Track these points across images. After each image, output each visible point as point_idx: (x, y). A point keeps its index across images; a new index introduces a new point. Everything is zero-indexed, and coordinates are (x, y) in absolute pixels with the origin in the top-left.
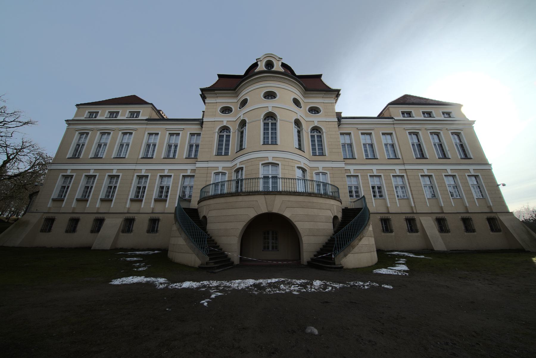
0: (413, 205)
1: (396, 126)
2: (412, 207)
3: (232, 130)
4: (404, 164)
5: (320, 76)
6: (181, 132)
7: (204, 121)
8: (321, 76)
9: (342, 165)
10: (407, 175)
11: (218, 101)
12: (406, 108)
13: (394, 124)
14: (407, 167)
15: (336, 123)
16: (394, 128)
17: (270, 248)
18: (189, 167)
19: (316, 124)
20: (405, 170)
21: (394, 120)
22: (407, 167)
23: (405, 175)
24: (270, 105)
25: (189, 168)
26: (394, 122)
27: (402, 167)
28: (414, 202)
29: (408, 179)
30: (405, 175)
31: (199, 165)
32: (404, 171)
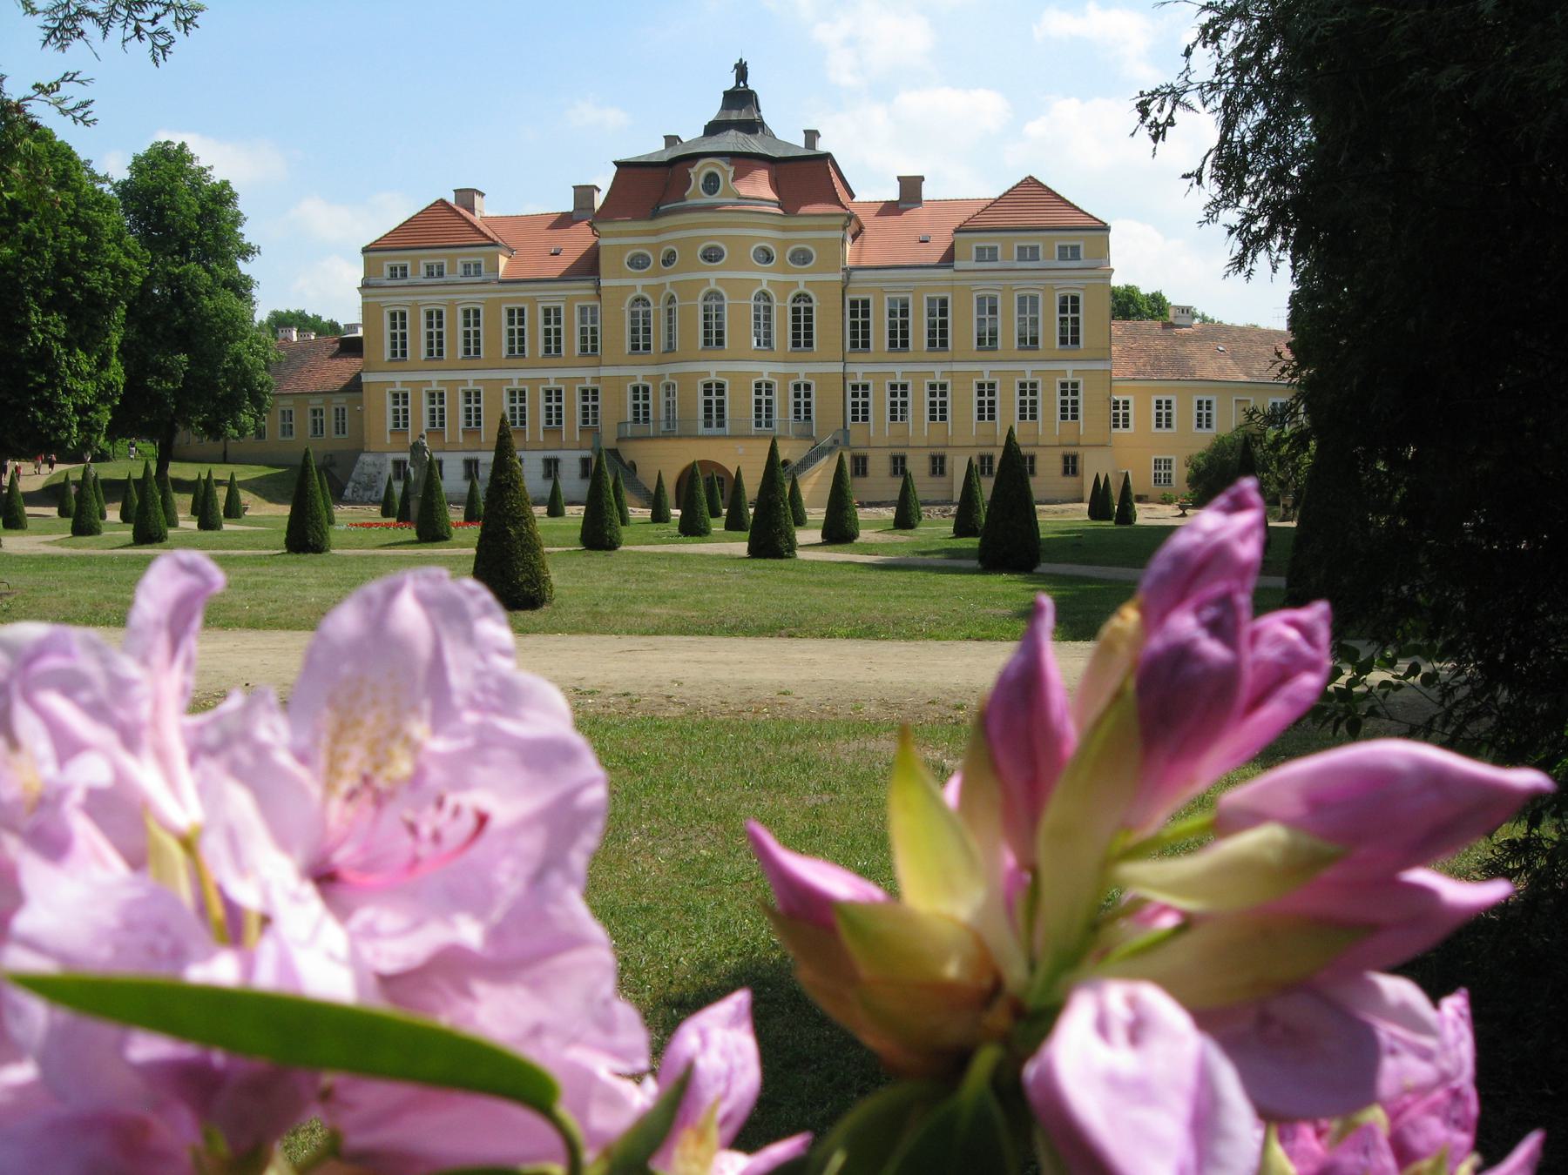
1: (956, 283)
7: (602, 285)
10: (952, 383)
12: (986, 240)
15: (840, 286)
16: (953, 286)
18: (588, 373)
19: (802, 289)
21: (952, 270)
22: (956, 367)
23: (949, 381)
24: (713, 276)
25: (586, 375)
27: (947, 367)
28: (952, 429)
30: (949, 381)
31: (605, 372)
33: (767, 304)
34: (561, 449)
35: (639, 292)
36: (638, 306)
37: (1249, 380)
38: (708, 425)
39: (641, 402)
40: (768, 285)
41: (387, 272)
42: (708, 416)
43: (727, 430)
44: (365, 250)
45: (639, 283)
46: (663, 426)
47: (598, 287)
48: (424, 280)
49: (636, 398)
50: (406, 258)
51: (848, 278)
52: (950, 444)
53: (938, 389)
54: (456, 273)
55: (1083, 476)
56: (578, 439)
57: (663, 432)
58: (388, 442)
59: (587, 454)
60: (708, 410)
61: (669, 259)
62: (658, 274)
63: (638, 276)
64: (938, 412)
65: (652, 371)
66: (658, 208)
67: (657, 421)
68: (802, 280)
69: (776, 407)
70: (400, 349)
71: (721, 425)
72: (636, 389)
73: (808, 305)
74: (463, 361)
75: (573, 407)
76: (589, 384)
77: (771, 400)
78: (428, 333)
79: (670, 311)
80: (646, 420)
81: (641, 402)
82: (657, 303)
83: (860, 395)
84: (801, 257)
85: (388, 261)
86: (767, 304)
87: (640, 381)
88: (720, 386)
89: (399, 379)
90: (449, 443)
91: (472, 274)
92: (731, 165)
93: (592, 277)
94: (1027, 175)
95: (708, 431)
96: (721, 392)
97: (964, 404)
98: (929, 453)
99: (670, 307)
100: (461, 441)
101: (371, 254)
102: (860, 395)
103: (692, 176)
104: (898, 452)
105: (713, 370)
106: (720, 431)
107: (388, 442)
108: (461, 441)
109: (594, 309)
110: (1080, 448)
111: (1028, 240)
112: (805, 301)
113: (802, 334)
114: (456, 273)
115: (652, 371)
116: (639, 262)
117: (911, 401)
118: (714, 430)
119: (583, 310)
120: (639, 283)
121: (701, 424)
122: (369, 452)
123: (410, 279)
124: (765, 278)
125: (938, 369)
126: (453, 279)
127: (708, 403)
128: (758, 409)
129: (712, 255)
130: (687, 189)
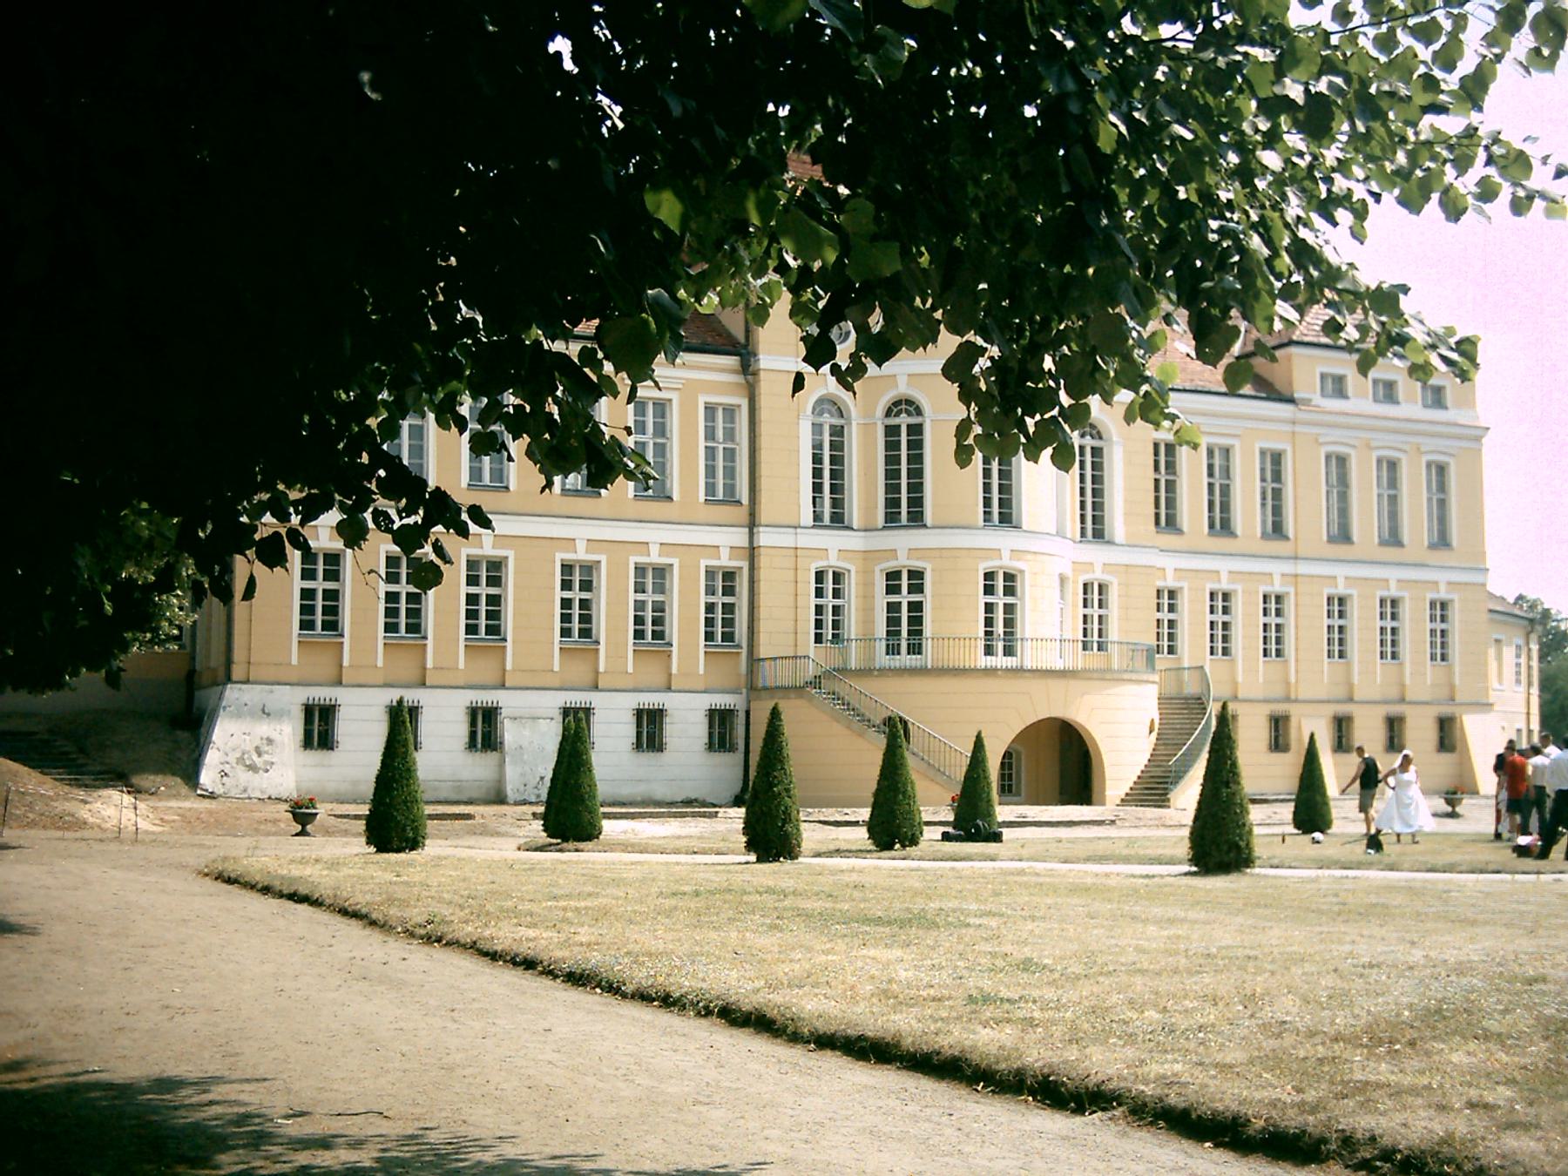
0: (1293, 680)
1: (1298, 429)
4: (1296, 558)
20: (1296, 576)
22: (1303, 568)
27: (1288, 568)
28: (1297, 671)
39: (829, 601)
53: (1275, 603)
59: (722, 701)
73: (1096, 443)
76: (725, 561)
77: (733, 605)
81: (829, 601)
87: (833, 561)
95: (990, 661)
98: (1384, 713)
99: (893, 421)
106: (1010, 662)
109: (730, 412)
119: (710, 410)
122: (247, 682)
125: (1277, 568)
128: (989, 622)
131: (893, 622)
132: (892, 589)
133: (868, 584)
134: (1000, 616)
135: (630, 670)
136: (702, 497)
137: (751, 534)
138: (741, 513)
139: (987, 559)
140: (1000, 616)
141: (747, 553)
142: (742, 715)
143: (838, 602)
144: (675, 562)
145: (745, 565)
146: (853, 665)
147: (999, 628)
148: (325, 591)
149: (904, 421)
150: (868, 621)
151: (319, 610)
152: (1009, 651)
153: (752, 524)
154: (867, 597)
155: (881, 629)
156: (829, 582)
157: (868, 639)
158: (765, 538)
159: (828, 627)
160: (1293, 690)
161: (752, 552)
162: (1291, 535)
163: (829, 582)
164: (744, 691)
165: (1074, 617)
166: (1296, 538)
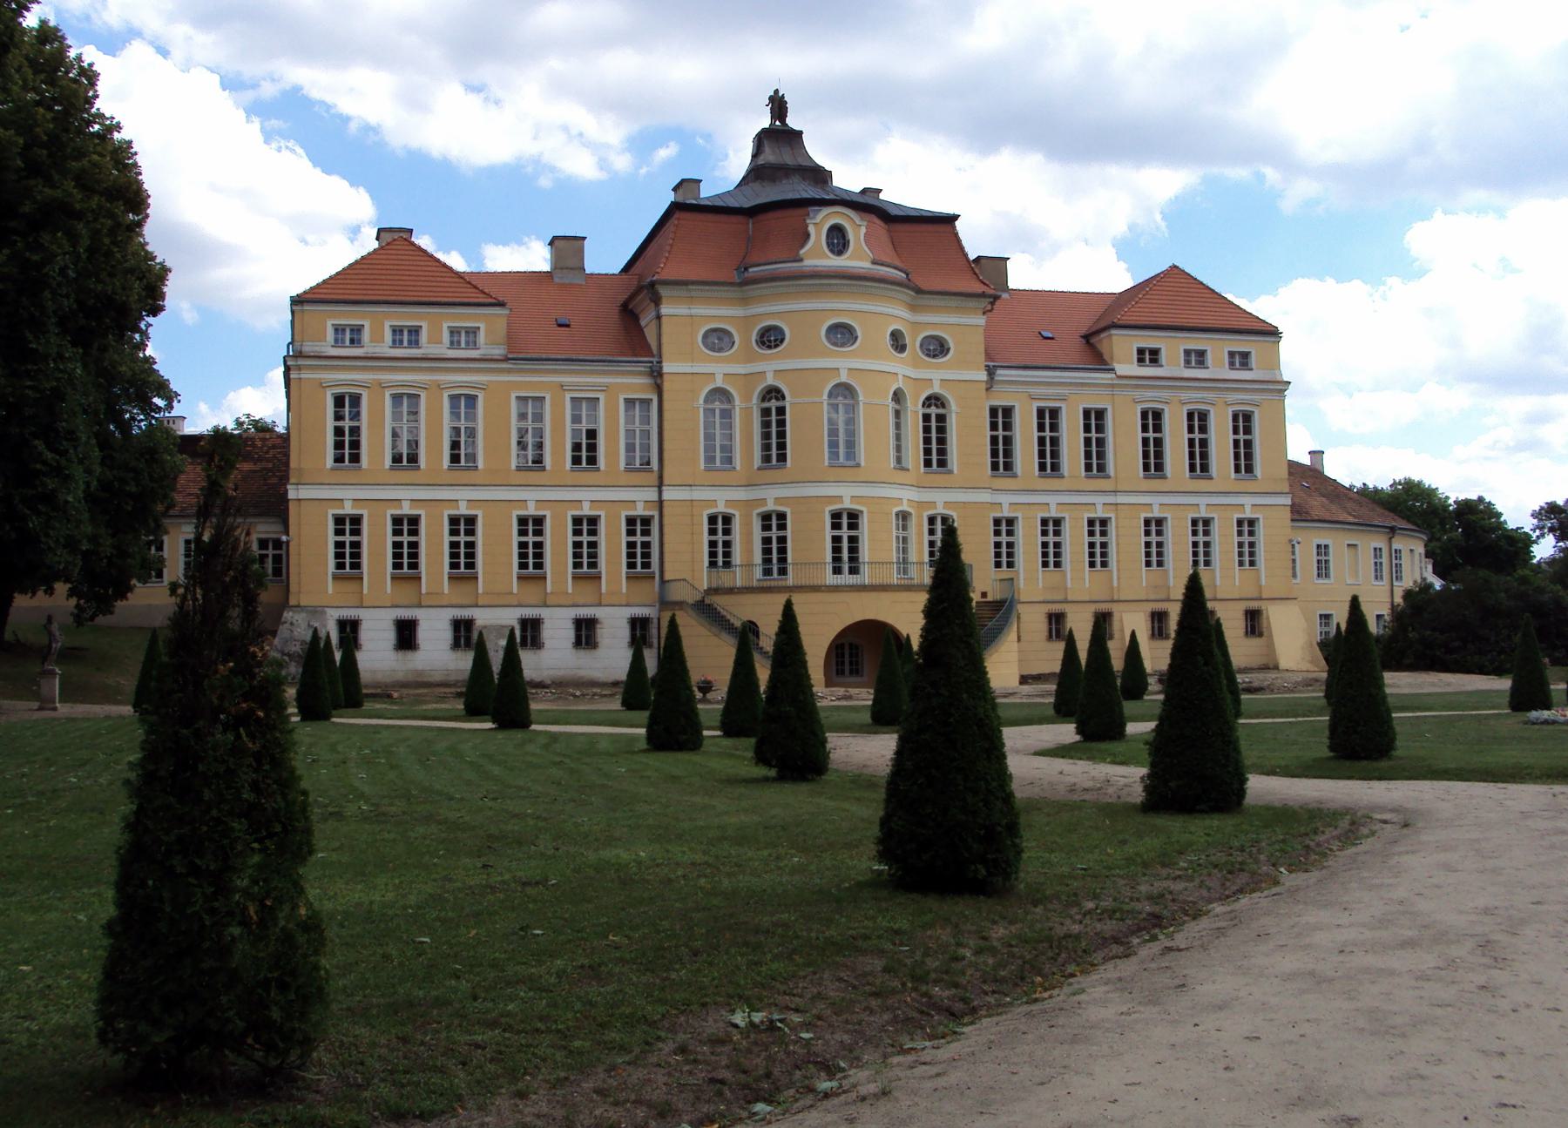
0: (1115, 584)
1: (1117, 391)
2: (1112, 588)
3: (737, 402)
5: (952, 219)
6: (601, 396)
7: (665, 370)
8: (956, 217)
9: (985, 497)
10: (1117, 518)
11: (693, 312)
13: (1113, 386)
14: (1121, 499)
15: (984, 386)
17: (847, 672)
19: (937, 389)
21: (1114, 376)
22: (1121, 499)
24: (844, 364)
25: (640, 499)
26: (1115, 382)
27: (1110, 499)
29: (1117, 527)
32: (1113, 507)
33: (897, 407)
34: (600, 605)
35: (719, 383)
36: (769, 400)
37: (1356, 520)
38: (837, 571)
39: (720, 538)
40: (941, 386)
41: (330, 335)
42: (837, 559)
43: (866, 576)
44: (297, 301)
45: (719, 369)
46: (758, 573)
47: (657, 374)
48: (392, 350)
49: (713, 532)
50: (477, 317)
51: (992, 379)
52: (1116, 598)
53: (1098, 526)
54: (441, 343)
55: (1271, 636)
56: (624, 590)
57: (759, 580)
58: (330, 591)
60: (837, 550)
61: (770, 338)
62: (750, 358)
63: (718, 361)
64: (1098, 556)
65: (741, 494)
66: (746, 269)
67: (749, 565)
68: (937, 375)
69: (602, 550)
70: (348, 448)
71: (854, 571)
72: (712, 520)
73: (941, 411)
74: (760, 472)
75: (612, 544)
76: (640, 511)
78: (1057, 431)
79: (766, 412)
80: (727, 564)
81: (720, 538)
82: (747, 398)
83: (348, 532)
84: (936, 348)
85: (330, 319)
86: (726, 406)
87: (721, 508)
88: (854, 517)
89: (348, 498)
90: (427, 594)
91: (463, 345)
92: (862, 219)
93: (651, 359)
94: (1171, 264)
96: (853, 526)
97: (1126, 542)
99: (766, 405)
100: (446, 591)
101: (307, 307)
102: (348, 532)
103: (811, 229)
104: (1056, 608)
105: (847, 495)
107: (330, 591)
108: (446, 591)
110: (1170, 603)
111: (1196, 342)
112: (937, 406)
113: (936, 453)
114: (441, 343)
115: (741, 494)
116: (718, 339)
117: (1021, 541)
118: (846, 579)
120: (719, 369)
121: (829, 569)
123: (368, 348)
124: (903, 370)
125: (1099, 500)
126: (377, 350)
127: (837, 540)
129: (842, 334)
130: (802, 246)
131: (767, 551)
132: (767, 528)
133: (747, 525)
134: (845, 545)
135: (570, 591)
136: (622, 465)
137: (660, 493)
138: (653, 479)
139: (830, 503)
140: (845, 545)
141: (657, 504)
142: (655, 621)
143: (727, 538)
144: (602, 514)
145: (656, 513)
146: (739, 584)
147: (845, 555)
148: (409, 542)
149: (773, 404)
150: (748, 551)
151: (531, 555)
152: (854, 571)
153: (660, 486)
154: (748, 535)
155: (758, 557)
156: (720, 523)
157: (749, 565)
158: (668, 494)
159: (720, 555)
160: (1115, 591)
161: (661, 502)
162: (1112, 473)
163: (720, 523)
164: (657, 605)
165: (920, 543)
166: (1116, 478)
